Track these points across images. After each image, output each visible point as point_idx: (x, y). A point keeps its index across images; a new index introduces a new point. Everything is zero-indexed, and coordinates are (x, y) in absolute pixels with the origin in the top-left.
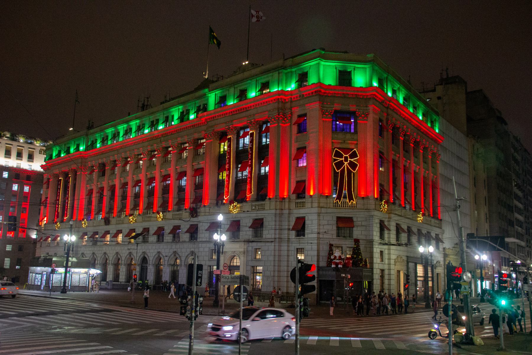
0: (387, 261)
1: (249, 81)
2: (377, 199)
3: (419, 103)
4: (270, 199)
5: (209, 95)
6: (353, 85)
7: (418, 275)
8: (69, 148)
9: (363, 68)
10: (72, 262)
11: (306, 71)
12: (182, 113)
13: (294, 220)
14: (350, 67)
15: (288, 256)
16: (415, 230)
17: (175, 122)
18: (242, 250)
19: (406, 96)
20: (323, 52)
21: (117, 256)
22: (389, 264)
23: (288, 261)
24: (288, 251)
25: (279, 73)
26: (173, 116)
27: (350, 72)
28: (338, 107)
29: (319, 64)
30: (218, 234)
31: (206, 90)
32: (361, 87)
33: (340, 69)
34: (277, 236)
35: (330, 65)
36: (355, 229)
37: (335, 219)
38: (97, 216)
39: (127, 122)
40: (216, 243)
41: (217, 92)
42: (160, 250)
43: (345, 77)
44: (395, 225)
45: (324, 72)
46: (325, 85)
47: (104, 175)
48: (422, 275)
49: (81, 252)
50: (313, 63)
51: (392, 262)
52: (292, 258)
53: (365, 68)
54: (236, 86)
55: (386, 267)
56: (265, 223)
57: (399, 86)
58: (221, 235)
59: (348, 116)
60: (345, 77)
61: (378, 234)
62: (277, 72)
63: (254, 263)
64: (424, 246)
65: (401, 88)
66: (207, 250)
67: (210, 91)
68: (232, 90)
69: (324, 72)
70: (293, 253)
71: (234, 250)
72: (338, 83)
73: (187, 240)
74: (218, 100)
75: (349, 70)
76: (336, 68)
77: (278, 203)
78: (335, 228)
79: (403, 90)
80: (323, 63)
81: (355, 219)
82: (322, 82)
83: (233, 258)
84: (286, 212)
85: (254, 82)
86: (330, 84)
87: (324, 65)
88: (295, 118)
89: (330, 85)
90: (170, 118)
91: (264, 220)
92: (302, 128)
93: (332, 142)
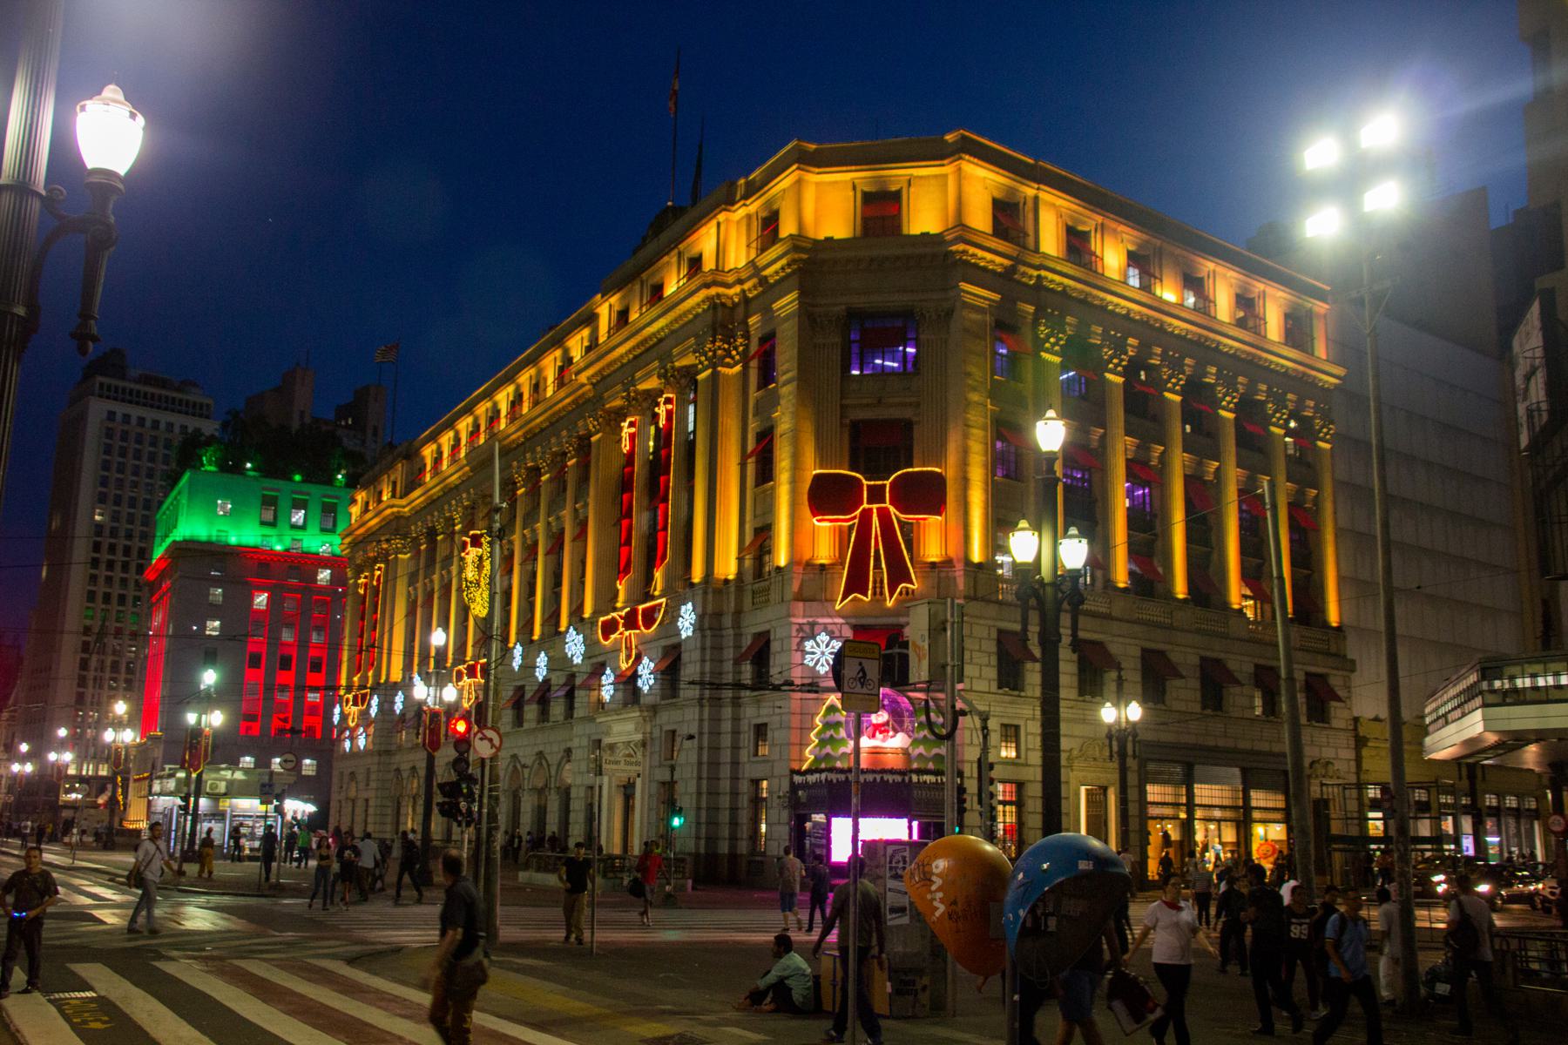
1: (666, 259)
6: (905, 232)
7: (1197, 801)
8: (380, 493)
9: (936, 176)
10: (230, 783)
11: (775, 207)
14: (897, 174)
15: (736, 748)
16: (1241, 665)
17: (549, 393)
18: (639, 737)
19: (1140, 246)
20: (813, 147)
23: (735, 763)
24: (736, 733)
25: (719, 224)
26: (545, 379)
27: (897, 196)
28: (859, 301)
29: (799, 182)
35: (836, 182)
41: (613, 300)
42: (516, 751)
43: (881, 209)
45: (824, 203)
46: (816, 242)
48: (1226, 802)
50: (785, 182)
52: (744, 756)
53: (945, 176)
54: (644, 276)
56: (685, 657)
57: (1099, 219)
59: (899, 323)
60: (881, 209)
61: (992, 673)
62: (714, 222)
64: (1116, 705)
65: (1108, 223)
66: (585, 742)
68: (637, 287)
69: (824, 203)
70: (747, 738)
71: (624, 739)
72: (858, 233)
73: (561, 718)
74: (614, 316)
75: (893, 188)
76: (854, 188)
77: (710, 597)
79: (1121, 228)
80: (816, 178)
82: (811, 234)
84: (727, 621)
85: (672, 258)
86: (829, 235)
87: (818, 184)
88: (754, 346)
89: (829, 240)
92: (767, 375)
93: (842, 406)
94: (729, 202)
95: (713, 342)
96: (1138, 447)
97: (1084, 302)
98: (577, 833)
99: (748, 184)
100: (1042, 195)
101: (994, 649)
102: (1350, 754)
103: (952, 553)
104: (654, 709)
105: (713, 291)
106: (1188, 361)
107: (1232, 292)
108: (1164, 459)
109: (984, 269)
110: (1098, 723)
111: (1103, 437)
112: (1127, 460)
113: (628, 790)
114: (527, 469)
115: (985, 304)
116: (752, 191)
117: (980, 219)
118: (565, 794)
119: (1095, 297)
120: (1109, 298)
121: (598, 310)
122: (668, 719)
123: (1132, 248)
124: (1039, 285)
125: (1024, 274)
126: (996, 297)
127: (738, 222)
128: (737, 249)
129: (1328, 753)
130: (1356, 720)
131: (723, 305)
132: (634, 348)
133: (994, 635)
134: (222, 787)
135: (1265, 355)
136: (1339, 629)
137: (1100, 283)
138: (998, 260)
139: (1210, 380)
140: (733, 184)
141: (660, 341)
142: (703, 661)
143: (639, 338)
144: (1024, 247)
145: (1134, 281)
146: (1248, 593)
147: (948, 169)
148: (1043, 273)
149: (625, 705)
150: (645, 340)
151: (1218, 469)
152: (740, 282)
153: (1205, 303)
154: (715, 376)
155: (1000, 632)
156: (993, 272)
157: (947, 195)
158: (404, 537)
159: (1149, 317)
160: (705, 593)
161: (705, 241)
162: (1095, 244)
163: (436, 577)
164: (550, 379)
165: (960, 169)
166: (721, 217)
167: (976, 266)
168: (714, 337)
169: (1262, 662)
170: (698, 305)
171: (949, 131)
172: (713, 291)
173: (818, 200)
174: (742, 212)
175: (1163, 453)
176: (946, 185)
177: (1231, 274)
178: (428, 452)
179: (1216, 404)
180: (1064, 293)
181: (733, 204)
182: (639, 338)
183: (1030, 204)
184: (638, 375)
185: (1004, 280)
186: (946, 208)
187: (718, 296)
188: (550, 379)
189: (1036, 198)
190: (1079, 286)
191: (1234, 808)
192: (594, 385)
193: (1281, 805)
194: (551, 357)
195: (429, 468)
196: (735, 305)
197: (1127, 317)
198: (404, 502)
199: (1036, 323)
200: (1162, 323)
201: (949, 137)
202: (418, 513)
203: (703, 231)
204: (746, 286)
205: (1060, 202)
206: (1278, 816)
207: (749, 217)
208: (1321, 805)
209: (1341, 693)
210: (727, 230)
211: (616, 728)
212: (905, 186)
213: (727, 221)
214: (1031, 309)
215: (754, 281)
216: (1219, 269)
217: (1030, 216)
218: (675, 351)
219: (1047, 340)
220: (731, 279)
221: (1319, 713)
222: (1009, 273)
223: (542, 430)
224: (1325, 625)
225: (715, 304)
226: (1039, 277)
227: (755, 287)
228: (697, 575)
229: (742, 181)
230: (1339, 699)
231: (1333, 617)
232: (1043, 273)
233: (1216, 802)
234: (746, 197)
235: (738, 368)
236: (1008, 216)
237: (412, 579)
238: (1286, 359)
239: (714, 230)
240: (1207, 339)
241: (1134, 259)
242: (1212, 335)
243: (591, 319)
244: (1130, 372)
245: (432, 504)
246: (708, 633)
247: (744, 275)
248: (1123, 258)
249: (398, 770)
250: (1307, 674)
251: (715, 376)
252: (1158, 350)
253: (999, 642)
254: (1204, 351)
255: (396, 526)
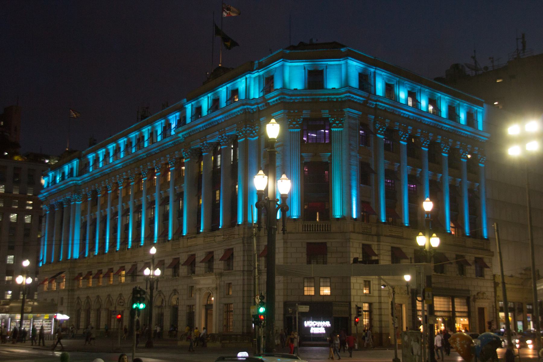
0: (376, 293)
2: (355, 219)
3: (439, 95)
4: (239, 225)
5: (186, 106)
11: (271, 74)
12: (165, 128)
13: (263, 249)
17: (159, 139)
18: (214, 286)
21: (109, 299)
22: (380, 296)
25: (246, 78)
26: (157, 132)
29: (283, 66)
30: (150, 269)
31: (185, 100)
32: (333, 88)
33: (309, 69)
34: (246, 269)
36: (329, 255)
37: (305, 245)
38: (91, 253)
39: (115, 140)
40: (148, 278)
41: (193, 103)
43: (315, 79)
44: (390, 248)
47: (97, 204)
48: (446, 309)
49: (76, 297)
50: (277, 65)
51: (383, 294)
53: (341, 65)
55: (375, 300)
57: (398, 79)
58: (155, 269)
60: (315, 79)
62: (244, 77)
63: (227, 301)
65: (401, 80)
67: (188, 101)
71: (207, 286)
74: (194, 110)
76: (305, 69)
78: (305, 255)
80: (288, 64)
81: (328, 245)
82: (288, 87)
83: (209, 296)
87: (290, 66)
89: (296, 89)
90: (154, 134)
91: (234, 250)
94: (250, 70)
95: (246, 127)
96: (412, 170)
97: (393, 113)
98: (182, 326)
99: (259, 63)
100: (377, 71)
101: (361, 252)
102: (493, 290)
103: (345, 214)
104: (221, 275)
105: (245, 107)
106: (430, 134)
107: (447, 105)
108: (421, 174)
109: (356, 102)
110: (403, 281)
111: (400, 166)
112: (408, 175)
113: (208, 307)
114: (148, 169)
115: (356, 116)
116: (261, 66)
117: (354, 83)
118: (175, 309)
119: (396, 111)
120: (402, 111)
121: (186, 106)
122: (227, 279)
123: (409, 90)
124: (376, 108)
125: (370, 103)
126: (360, 113)
127: (255, 78)
128: (254, 89)
129: (484, 290)
130: (494, 276)
131: (249, 112)
132: (206, 125)
133: (361, 246)
134: (30, 309)
135: (459, 130)
136: (488, 239)
137: (398, 106)
138: (361, 98)
139: (439, 141)
140: (252, 63)
141: (219, 124)
142: (244, 256)
143: (209, 122)
144: (370, 93)
145: (410, 103)
146: (452, 225)
147: (342, 62)
148: (378, 103)
149: (206, 272)
150: (212, 122)
151: (442, 177)
152: (257, 104)
153: (437, 109)
154: (246, 141)
155: (363, 245)
156: (360, 104)
157: (341, 73)
158: (79, 194)
159: (416, 118)
160: (244, 228)
161: (241, 84)
162: (396, 90)
163: (98, 213)
164: (159, 132)
165: (347, 63)
166: (248, 76)
167: (353, 101)
168: (246, 125)
169: (459, 253)
170: (238, 111)
171: (343, 46)
172: (245, 107)
173: (290, 73)
174: (257, 74)
175: (421, 172)
176: (341, 69)
177: (447, 97)
178: (91, 157)
179: (441, 151)
180: (385, 110)
181: (253, 71)
182: (209, 122)
183: (372, 75)
184: (208, 136)
185: (363, 106)
186: (341, 78)
187: (248, 108)
188: (159, 132)
189: (375, 73)
190: (391, 107)
191: (449, 312)
192: (185, 138)
193: (466, 310)
194: (160, 122)
195: (91, 164)
196: (254, 112)
197: (408, 118)
198: (79, 179)
199: (375, 123)
200: (421, 120)
201: (342, 50)
202: (85, 183)
203: (239, 80)
204: (259, 106)
205: (383, 73)
206: (465, 315)
207: (259, 76)
208: (481, 311)
209: (488, 264)
210: (250, 81)
211: (202, 282)
212: (325, 68)
213: (250, 77)
214: (373, 117)
215: (264, 104)
216: (442, 96)
217: (372, 79)
218: (226, 129)
219: (379, 130)
220: (253, 102)
221: (480, 274)
222: (365, 102)
223: (156, 154)
224: (482, 237)
225: (245, 112)
226: (376, 104)
227: (263, 106)
228: (240, 221)
229: (257, 62)
230: (488, 267)
231: (485, 235)
232: (378, 103)
233: (442, 309)
234: (259, 68)
235: (257, 138)
236: (365, 80)
237: (83, 213)
238: (468, 132)
239: (244, 81)
240: (438, 125)
241: (411, 94)
242: (439, 124)
243: (182, 109)
244: (409, 140)
245: (94, 180)
246: (246, 244)
247: (259, 101)
248: (407, 94)
249: (78, 298)
250: (476, 258)
251: (246, 141)
252: (419, 131)
253: (363, 249)
254: (436, 129)
255: (76, 189)
